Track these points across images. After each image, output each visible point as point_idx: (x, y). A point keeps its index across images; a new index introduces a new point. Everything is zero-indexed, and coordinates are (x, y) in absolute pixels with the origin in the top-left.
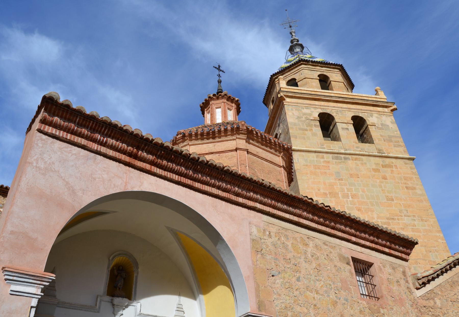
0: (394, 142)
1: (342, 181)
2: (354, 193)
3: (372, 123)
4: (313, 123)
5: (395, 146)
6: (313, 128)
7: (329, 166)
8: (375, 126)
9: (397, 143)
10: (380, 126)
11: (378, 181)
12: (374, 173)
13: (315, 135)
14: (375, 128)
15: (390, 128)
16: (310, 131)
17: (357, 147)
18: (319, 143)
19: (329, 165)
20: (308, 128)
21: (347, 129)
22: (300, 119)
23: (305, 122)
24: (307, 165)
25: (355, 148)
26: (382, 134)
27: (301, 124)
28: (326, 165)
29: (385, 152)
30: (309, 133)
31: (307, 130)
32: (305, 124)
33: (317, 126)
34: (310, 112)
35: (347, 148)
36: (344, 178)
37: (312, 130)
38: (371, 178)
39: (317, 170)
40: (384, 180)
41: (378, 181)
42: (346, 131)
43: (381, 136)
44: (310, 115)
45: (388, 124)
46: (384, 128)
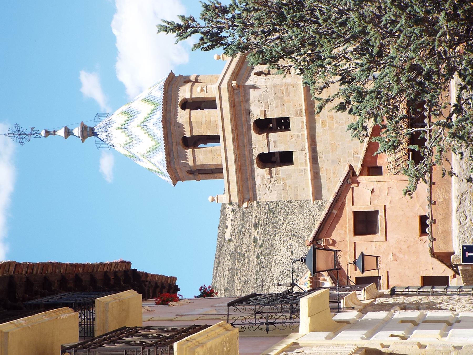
0: (283, 94)
1: (341, 160)
2: (352, 151)
3: (261, 114)
4: (274, 175)
5: (289, 95)
6: (281, 178)
7: (326, 169)
8: (265, 111)
9: (284, 91)
10: (264, 105)
11: (335, 125)
12: (327, 127)
13: (289, 177)
14: (268, 111)
15: (264, 93)
16: (285, 181)
17: (298, 136)
18: (299, 174)
19: (325, 169)
20: (282, 182)
21: (275, 142)
22: (271, 188)
23: (274, 184)
24: (329, 189)
25: (300, 139)
26: (274, 105)
27: (278, 188)
28: (325, 172)
29: (298, 109)
30: (288, 182)
31: (285, 184)
32: (276, 184)
33: (276, 171)
34: (259, 177)
35: (301, 148)
36: (337, 157)
37: (283, 179)
38: (333, 131)
39: (332, 181)
40: (334, 120)
41: (335, 125)
42: (278, 143)
43: (277, 107)
44: (263, 178)
45: (259, 96)
46: (265, 102)
